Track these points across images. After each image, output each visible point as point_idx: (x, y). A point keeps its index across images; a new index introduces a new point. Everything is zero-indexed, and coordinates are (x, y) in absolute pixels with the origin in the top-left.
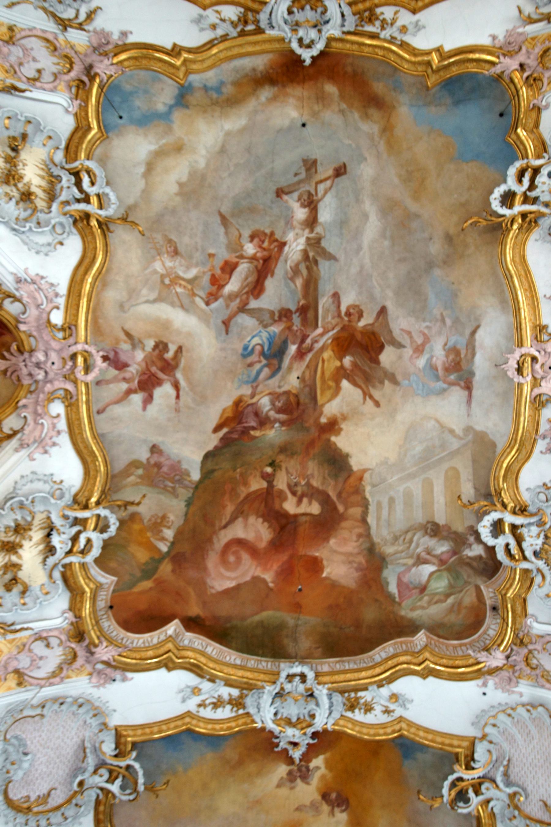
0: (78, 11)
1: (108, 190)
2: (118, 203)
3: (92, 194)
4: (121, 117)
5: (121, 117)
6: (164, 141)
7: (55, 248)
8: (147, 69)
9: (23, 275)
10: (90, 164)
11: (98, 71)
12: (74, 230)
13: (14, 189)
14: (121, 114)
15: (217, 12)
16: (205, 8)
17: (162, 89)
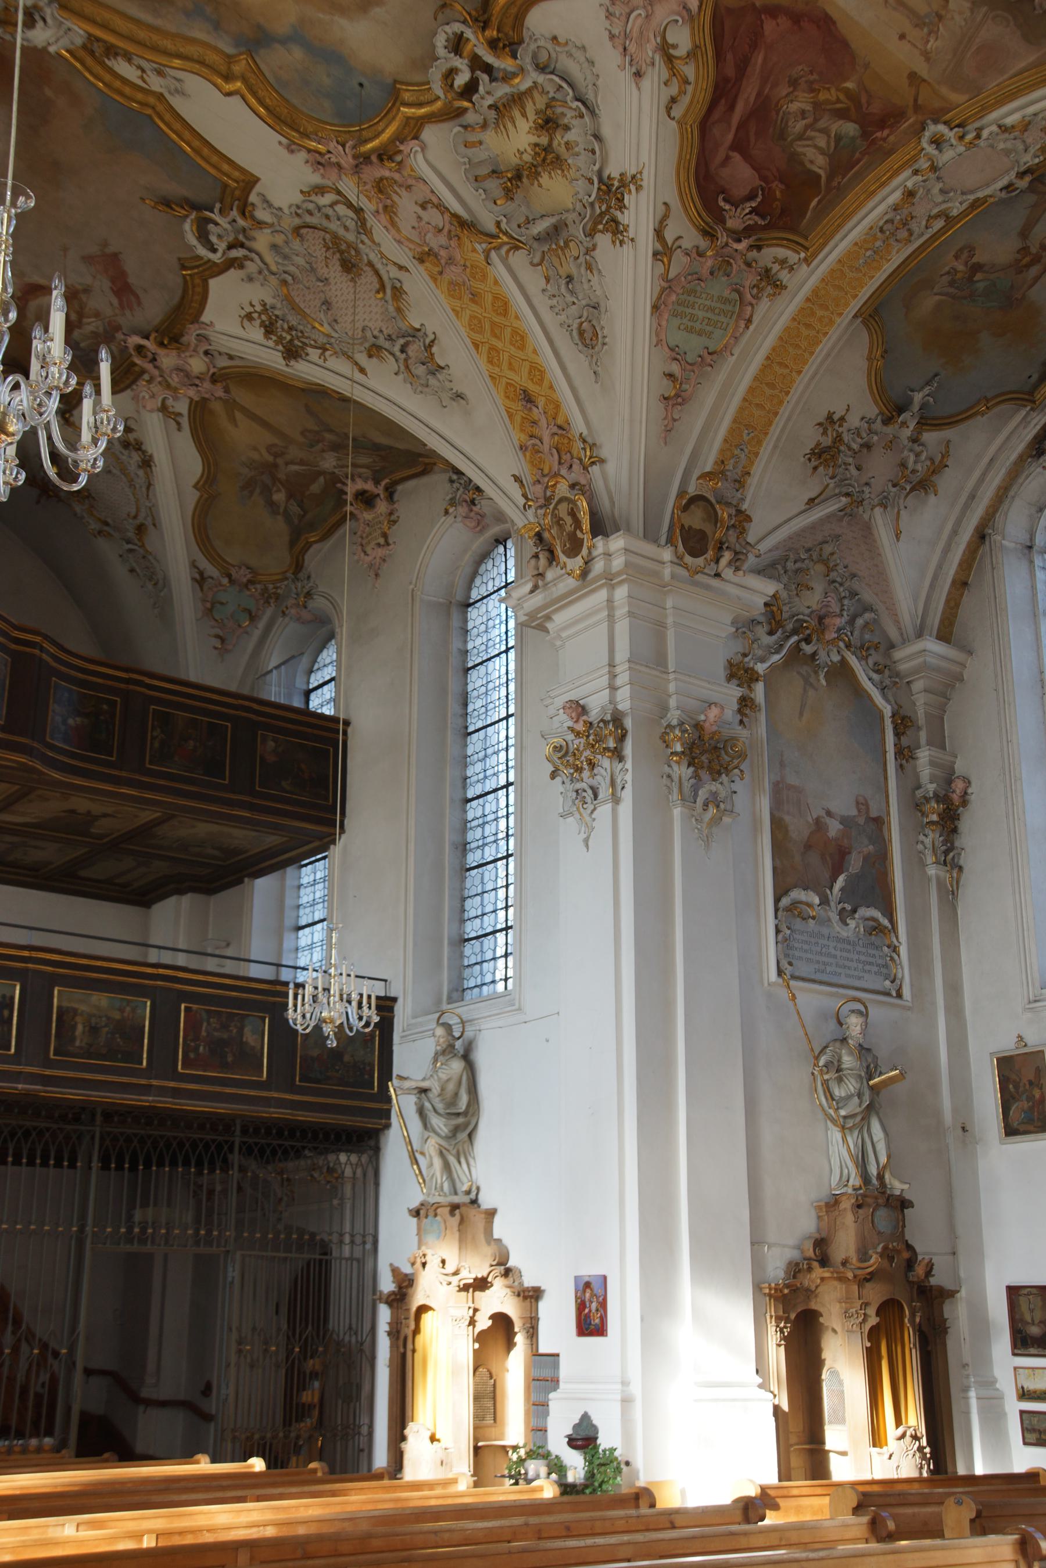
0: (331, 206)
1: (441, 52)
2: (440, 30)
3: (466, 61)
4: (361, 85)
5: (361, 85)
6: (321, 16)
7: (567, 43)
8: (287, 101)
9: (629, 71)
10: (438, 89)
11: (351, 160)
12: (526, 34)
13: (555, 143)
14: (358, 88)
15: (145, 81)
16: (160, 97)
17: (280, 68)
